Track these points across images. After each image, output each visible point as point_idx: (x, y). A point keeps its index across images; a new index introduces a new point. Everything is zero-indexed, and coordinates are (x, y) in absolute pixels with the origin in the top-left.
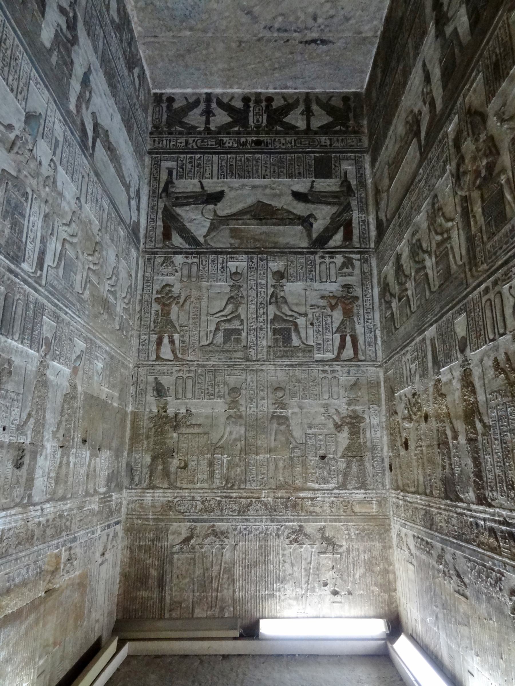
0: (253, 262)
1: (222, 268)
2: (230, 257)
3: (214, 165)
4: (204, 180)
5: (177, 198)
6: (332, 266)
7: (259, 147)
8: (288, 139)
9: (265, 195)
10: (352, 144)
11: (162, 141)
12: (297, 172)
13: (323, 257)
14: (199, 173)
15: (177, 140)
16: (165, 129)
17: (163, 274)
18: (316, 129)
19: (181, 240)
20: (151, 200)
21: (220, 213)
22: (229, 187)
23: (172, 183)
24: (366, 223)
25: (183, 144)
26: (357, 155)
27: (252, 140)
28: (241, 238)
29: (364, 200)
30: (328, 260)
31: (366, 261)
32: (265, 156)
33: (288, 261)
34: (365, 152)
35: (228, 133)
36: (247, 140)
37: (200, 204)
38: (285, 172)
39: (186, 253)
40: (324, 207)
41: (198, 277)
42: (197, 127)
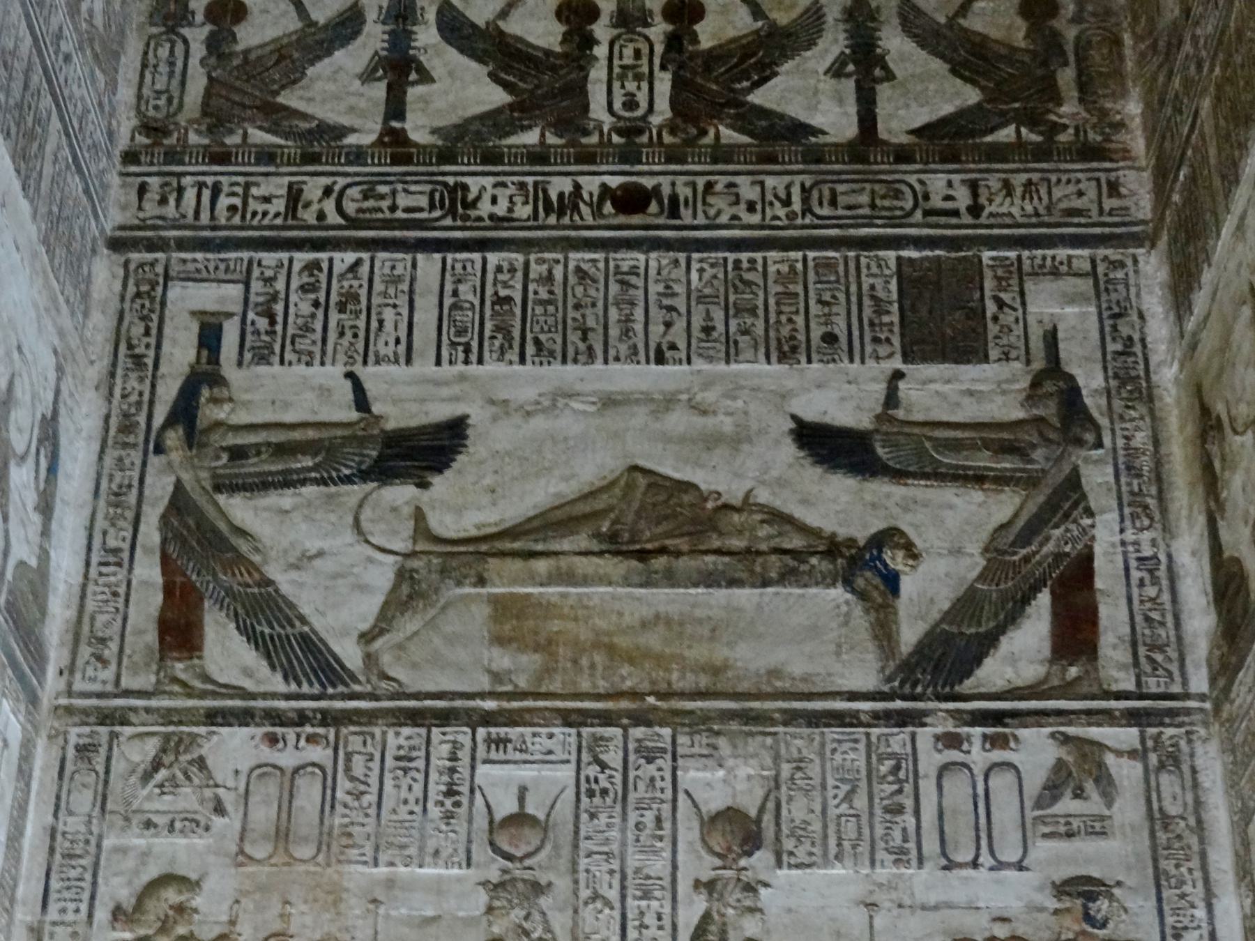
0: (603, 766)
1: (450, 792)
2: (489, 741)
3: (418, 302)
4: (371, 369)
5: (238, 453)
6: (1002, 784)
7: (636, 219)
8: (770, 182)
9: (666, 439)
10: (1077, 203)
11: (180, 190)
12: (817, 332)
13: (952, 741)
14: (345, 342)
15: (247, 186)
16: (193, 138)
17: (148, 824)
18: (905, 139)
19: (249, 656)
20: (108, 461)
21: (445, 524)
22: (492, 402)
23: (217, 380)
24: (1162, 572)
25: (279, 205)
26: (1101, 252)
27: (604, 186)
28: (546, 646)
29: (1146, 463)
30: (978, 756)
31: (1171, 760)
32: (666, 258)
33: (777, 758)
34: (1137, 240)
35: (492, 158)
36: (577, 187)
37: (348, 480)
38: (759, 329)
39: (275, 718)
40: (948, 494)
41: (323, 841)
42: (342, 131)
